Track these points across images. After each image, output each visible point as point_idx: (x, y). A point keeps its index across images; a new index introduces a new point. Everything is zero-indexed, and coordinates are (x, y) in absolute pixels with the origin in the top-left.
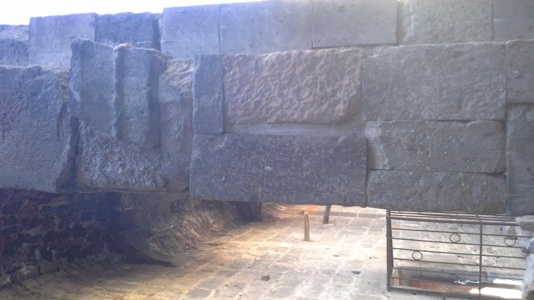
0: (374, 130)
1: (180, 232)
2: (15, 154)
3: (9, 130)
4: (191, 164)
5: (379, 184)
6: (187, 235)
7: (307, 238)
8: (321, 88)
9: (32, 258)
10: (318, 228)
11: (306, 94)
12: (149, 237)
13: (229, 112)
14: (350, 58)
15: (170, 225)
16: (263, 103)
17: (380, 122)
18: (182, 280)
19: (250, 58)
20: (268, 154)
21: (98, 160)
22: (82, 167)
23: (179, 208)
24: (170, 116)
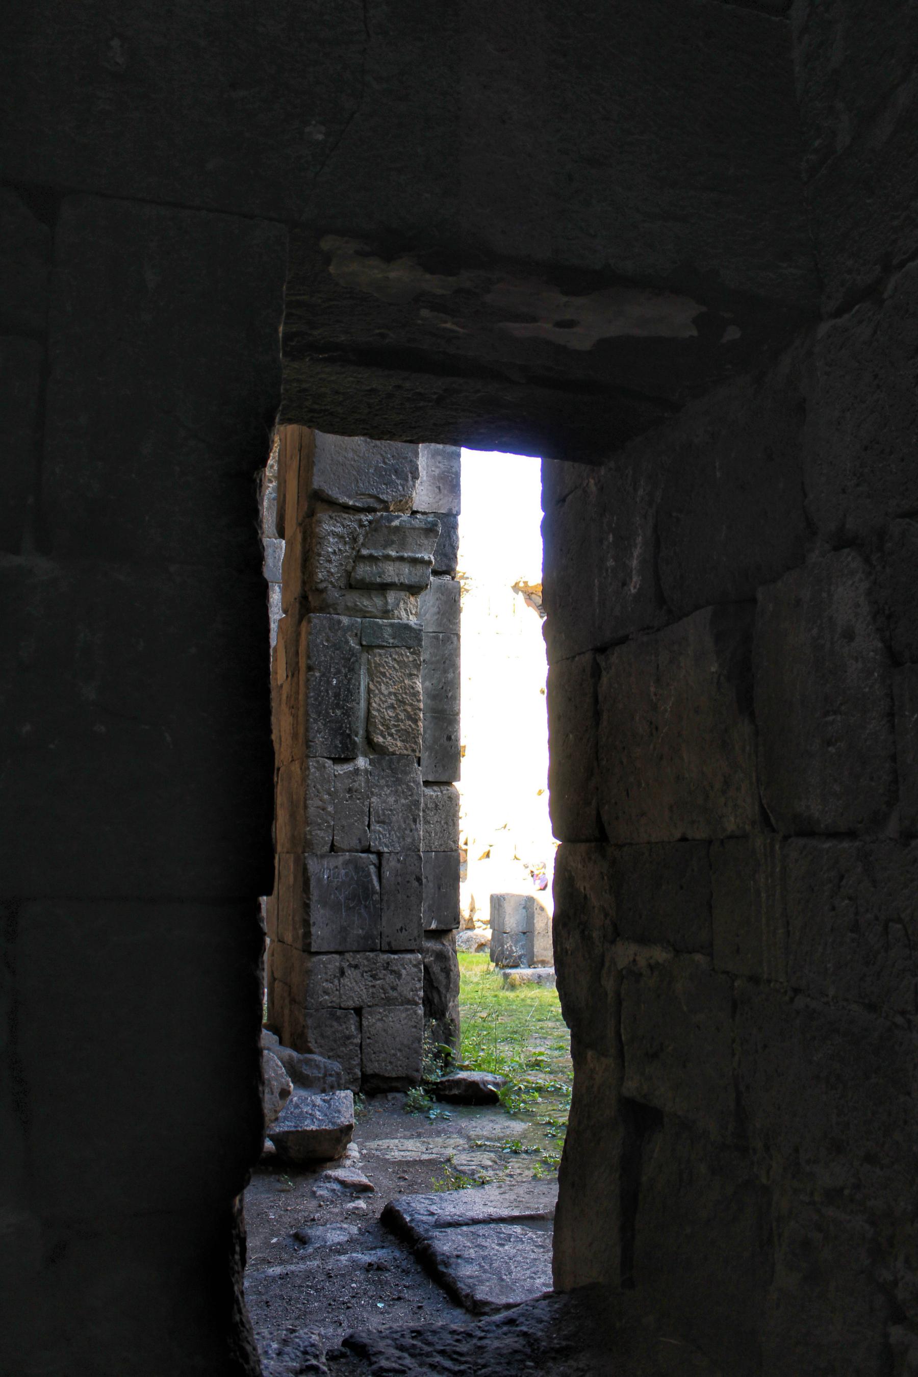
5: (324, 767)
8: (395, 726)
11: (391, 714)
14: (415, 747)
19: (419, 670)
20: (345, 682)
21: (339, 530)
22: (334, 512)
24: (375, 599)
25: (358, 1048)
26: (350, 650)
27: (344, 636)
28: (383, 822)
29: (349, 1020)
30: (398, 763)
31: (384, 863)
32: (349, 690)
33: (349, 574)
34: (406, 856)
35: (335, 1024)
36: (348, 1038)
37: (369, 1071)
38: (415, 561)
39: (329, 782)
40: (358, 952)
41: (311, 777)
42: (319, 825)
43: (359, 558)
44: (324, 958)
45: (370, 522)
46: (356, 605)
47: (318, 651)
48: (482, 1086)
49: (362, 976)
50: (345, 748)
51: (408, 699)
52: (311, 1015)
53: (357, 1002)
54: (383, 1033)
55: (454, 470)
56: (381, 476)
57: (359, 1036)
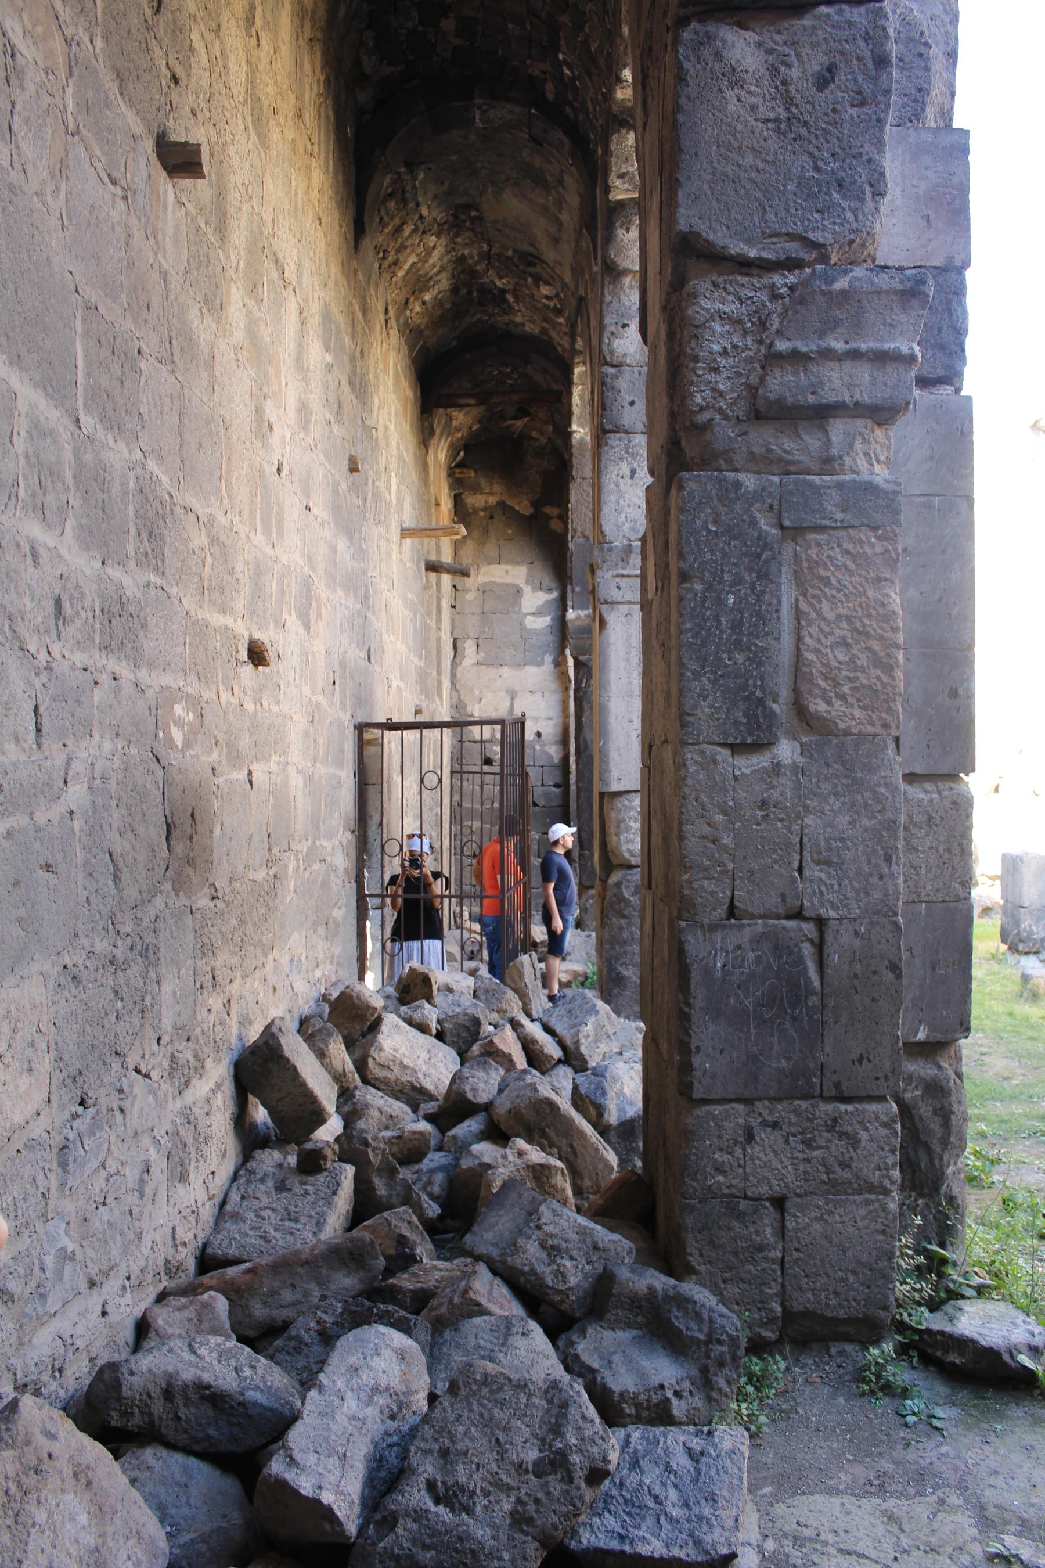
0: (789, 753)
1: (414, 231)
2: (736, 145)
3: (778, 130)
4: (732, 474)
5: (715, 762)
6: (406, 248)
8: (849, 678)
11: (841, 657)
14: (889, 718)
17: (801, 761)
18: (342, 280)
20: (752, 599)
21: (731, 307)
22: (720, 274)
23: (464, 221)
25: (776, 1267)
26: (759, 538)
27: (747, 511)
28: (828, 863)
29: (761, 1218)
30: (856, 750)
31: (829, 938)
32: (758, 614)
33: (753, 391)
34: (872, 923)
35: (736, 1224)
36: (760, 1248)
37: (797, 1307)
38: (881, 358)
40: (778, 1099)
41: (689, 781)
42: (706, 870)
43: (773, 359)
44: (717, 1110)
45: (792, 288)
46: (769, 451)
48: (1006, 1358)
49: (787, 1141)
50: (754, 723)
51: (873, 626)
52: (693, 1209)
53: (778, 1190)
54: (825, 1243)
57: (780, 1246)
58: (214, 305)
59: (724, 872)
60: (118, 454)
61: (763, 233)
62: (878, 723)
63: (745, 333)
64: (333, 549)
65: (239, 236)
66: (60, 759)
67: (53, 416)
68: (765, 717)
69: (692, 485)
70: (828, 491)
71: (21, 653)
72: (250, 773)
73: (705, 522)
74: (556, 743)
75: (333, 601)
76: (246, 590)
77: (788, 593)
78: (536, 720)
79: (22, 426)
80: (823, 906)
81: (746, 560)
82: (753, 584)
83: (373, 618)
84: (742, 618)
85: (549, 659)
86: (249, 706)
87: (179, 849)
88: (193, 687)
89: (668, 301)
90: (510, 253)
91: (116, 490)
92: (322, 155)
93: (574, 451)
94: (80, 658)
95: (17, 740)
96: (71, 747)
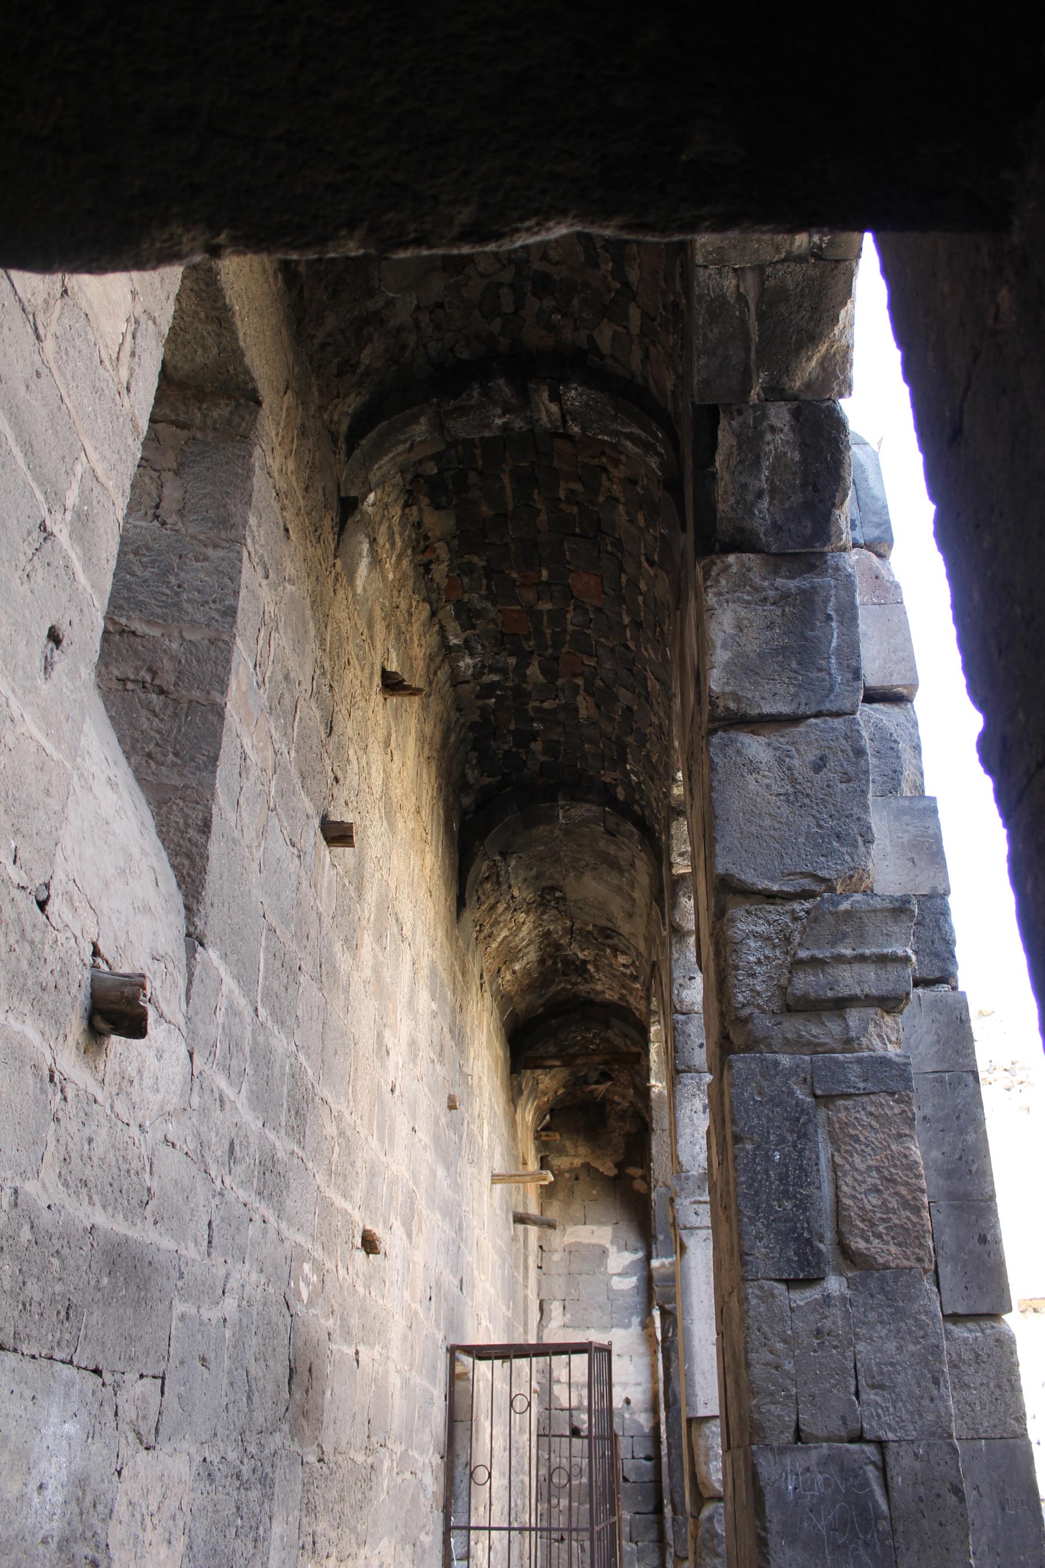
0: (837, 1286)
1: (506, 909)
5: (773, 1295)
6: (499, 923)
7: (496, 1179)
8: (883, 1219)
9: (486, 670)
10: (507, 1202)
11: (874, 1201)
12: (501, 854)
13: (841, 1102)
14: (922, 1253)
15: (519, 889)
16: (857, 1146)
17: (848, 1293)
18: (446, 944)
19: (911, 1126)
20: (795, 1155)
21: (762, 928)
22: (751, 905)
23: (550, 901)
26: (797, 1105)
27: (785, 1084)
28: (881, 1387)
31: (891, 1460)
32: (801, 1167)
33: (783, 989)
34: (929, 1445)
38: (883, 960)
39: (782, 1320)
41: (752, 1313)
42: (772, 1394)
43: (798, 964)
45: (808, 912)
47: (746, 1111)
50: (804, 1262)
51: (899, 1174)
55: (931, 832)
56: (817, 845)
58: (352, 945)
59: (789, 1397)
60: (281, 1043)
61: (782, 873)
62: (912, 1257)
63: (774, 947)
64: (434, 1173)
65: (371, 896)
66: (222, 1272)
67: (242, 1002)
68: (814, 1255)
69: (740, 1065)
70: (851, 1065)
71: (204, 1175)
72: (357, 1353)
73: (752, 1094)
74: (646, 1410)
75: (431, 1219)
76: (363, 1184)
77: (824, 1152)
78: (625, 1385)
79: (223, 1004)
80: (881, 1428)
81: (788, 1123)
82: (795, 1142)
83: (466, 1251)
84: (787, 1171)
85: (636, 1320)
86: (361, 1290)
87: (298, 1396)
88: (318, 1254)
89: (714, 928)
90: (590, 928)
91: (277, 1069)
92: (434, 843)
93: (653, 1104)
94: (242, 1195)
95: (196, 1243)
96: (229, 1265)
